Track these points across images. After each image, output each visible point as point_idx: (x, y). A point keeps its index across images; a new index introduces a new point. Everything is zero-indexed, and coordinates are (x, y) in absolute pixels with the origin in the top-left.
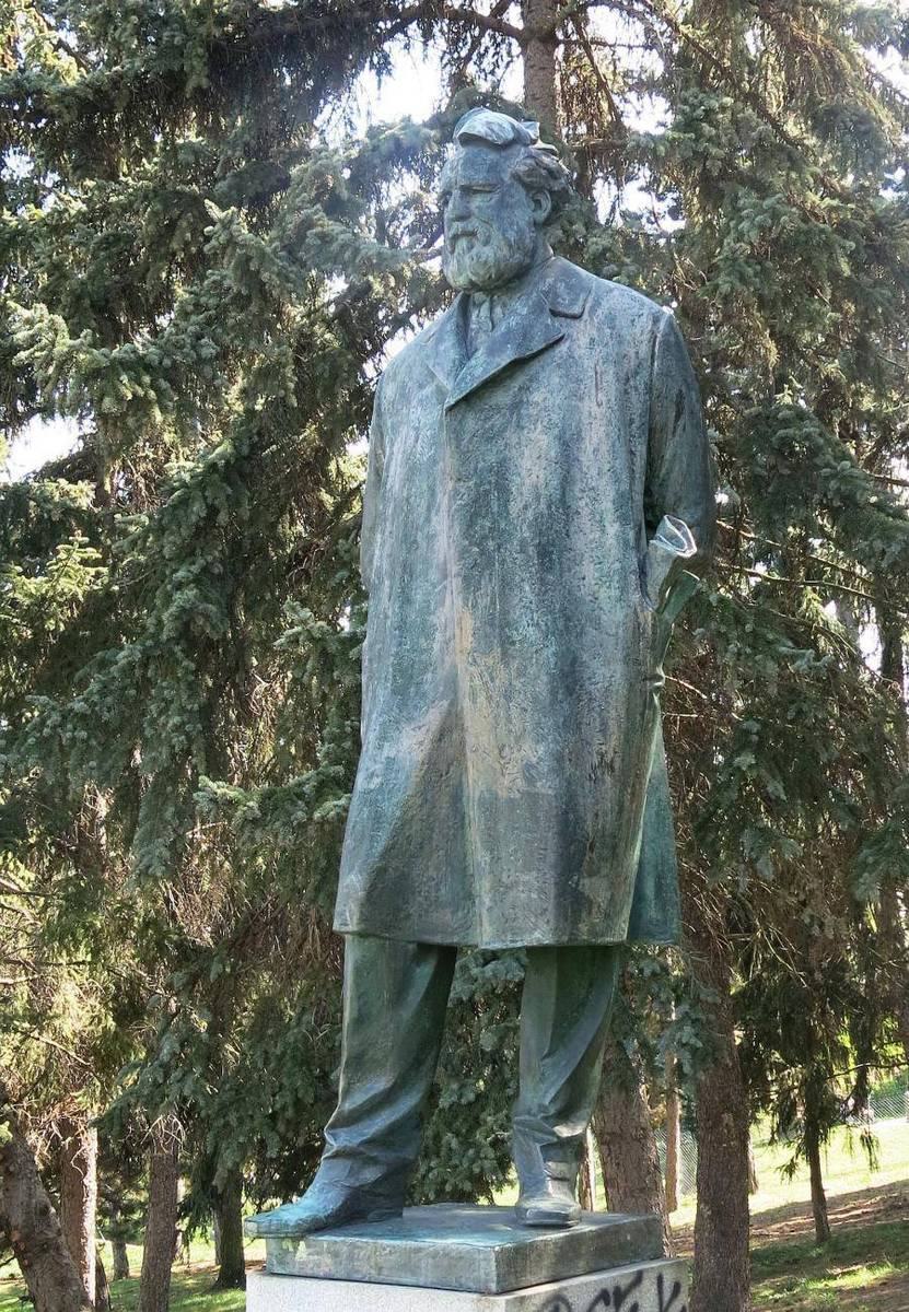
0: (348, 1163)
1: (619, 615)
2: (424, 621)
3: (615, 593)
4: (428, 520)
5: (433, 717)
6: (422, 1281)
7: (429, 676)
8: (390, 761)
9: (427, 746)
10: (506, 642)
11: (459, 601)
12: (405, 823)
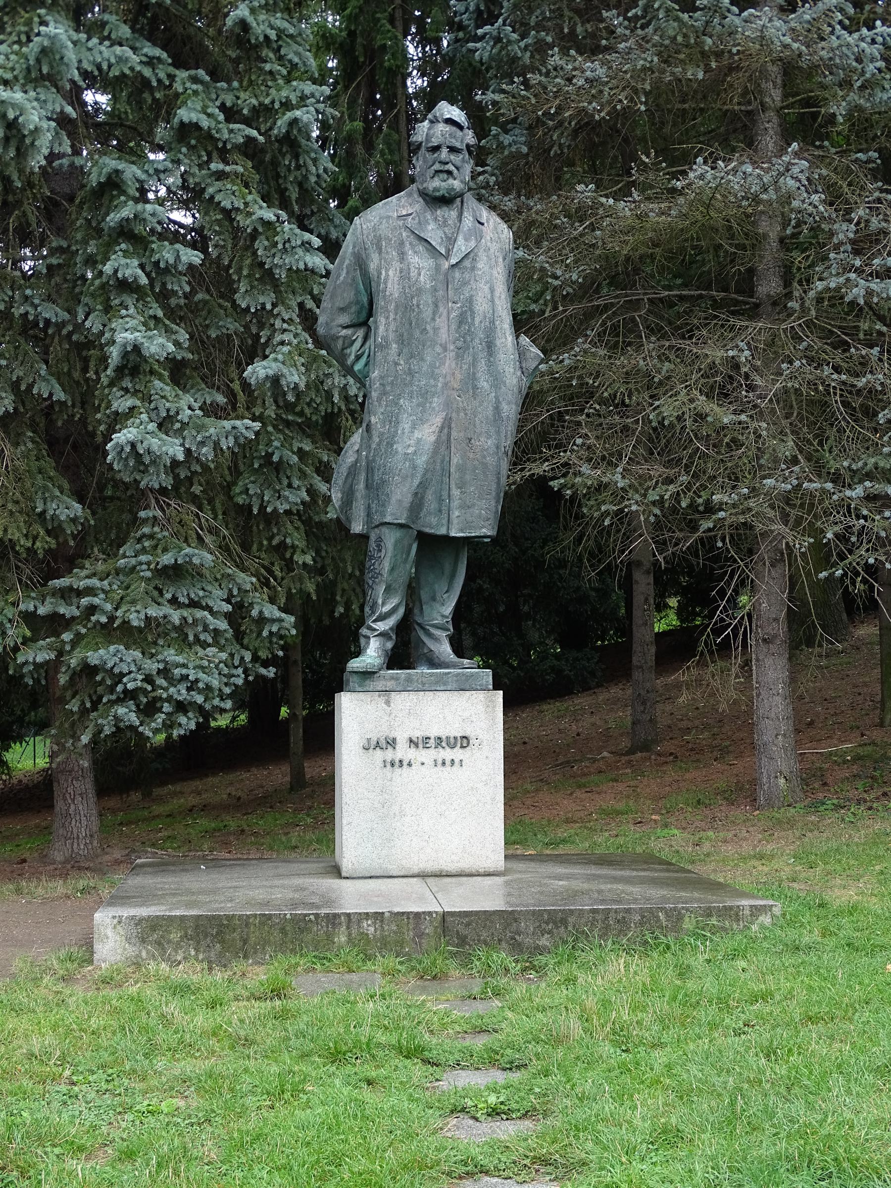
0: (381, 638)
1: (515, 381)
2: (433, 372)
3: (512, 370)
4: (433, 319)
5: (438, 420)
6: (449, 688)
7: (436, 399)
8: (419, 441)
9: (436, 434)
10: (475, 388)
11: (453, 365)
12: (426, 471)
